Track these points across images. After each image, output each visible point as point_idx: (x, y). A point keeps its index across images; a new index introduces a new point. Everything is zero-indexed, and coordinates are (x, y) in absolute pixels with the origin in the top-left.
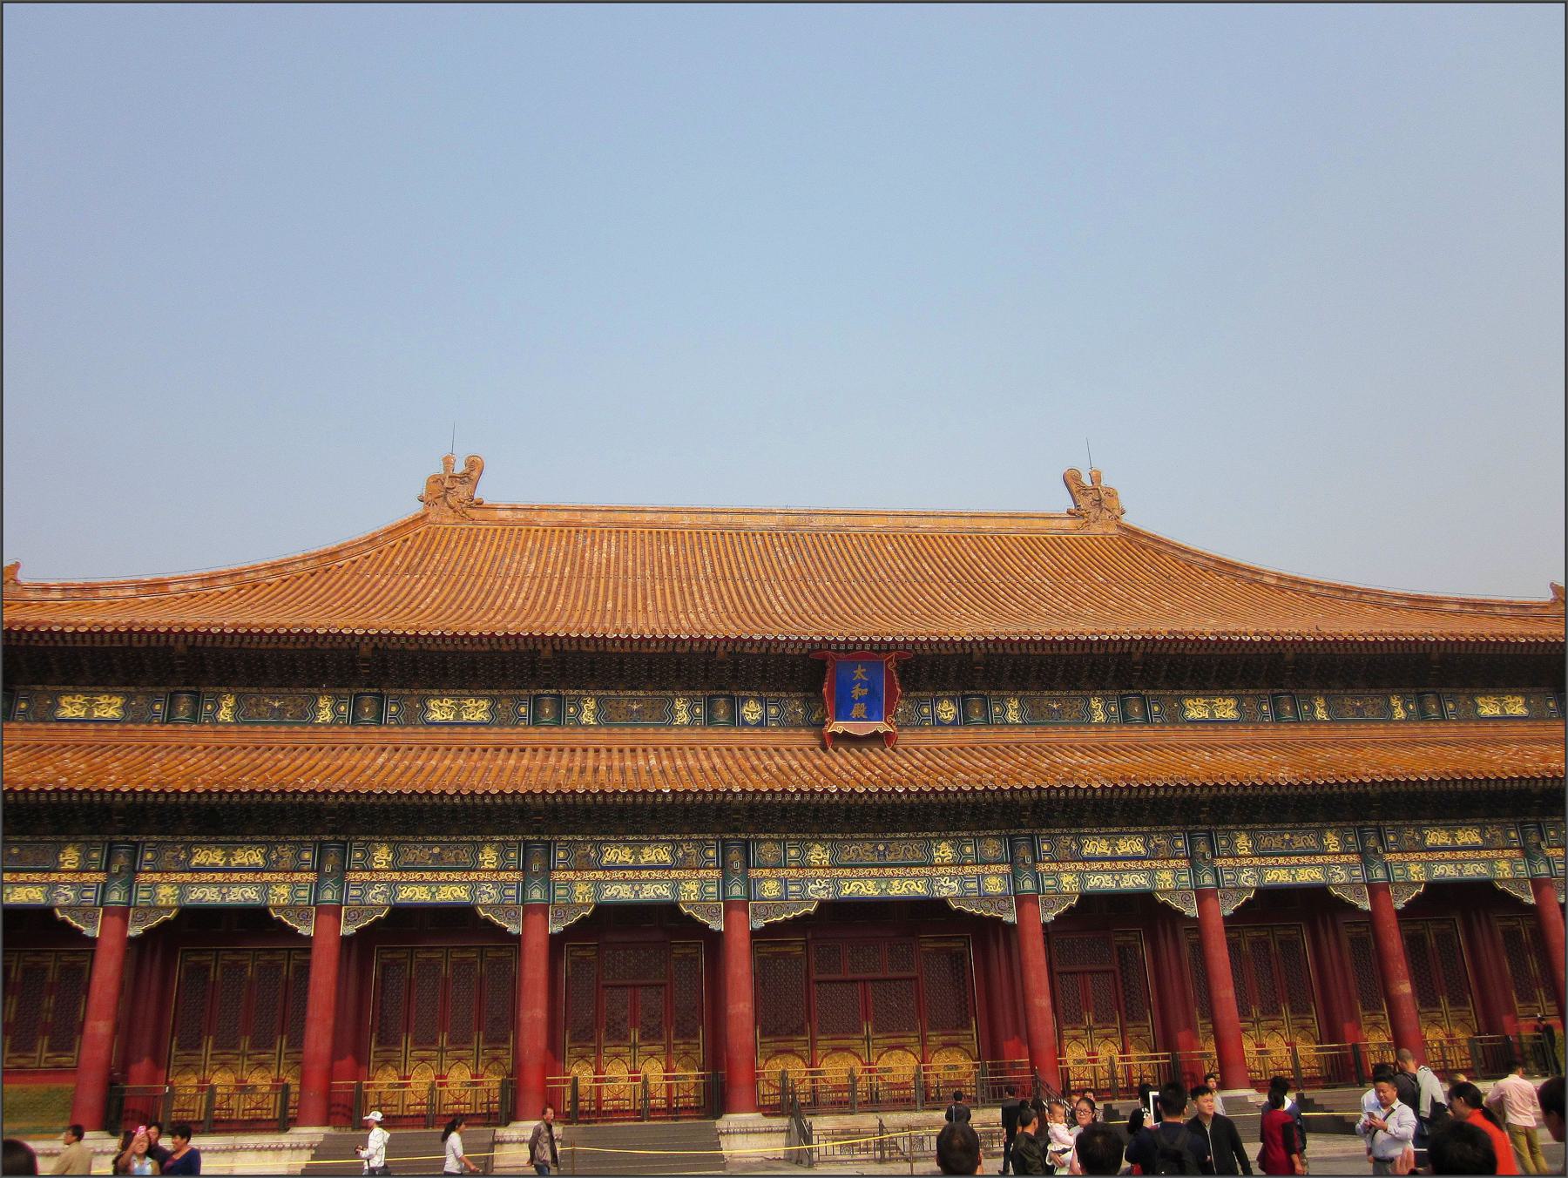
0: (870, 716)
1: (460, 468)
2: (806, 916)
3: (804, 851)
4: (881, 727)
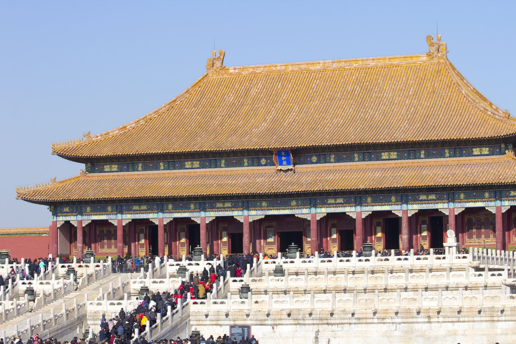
0: (289, 164)
1: (218, 55)
2: (262, 219)
3: (261, 204)
4: (291, 167)
